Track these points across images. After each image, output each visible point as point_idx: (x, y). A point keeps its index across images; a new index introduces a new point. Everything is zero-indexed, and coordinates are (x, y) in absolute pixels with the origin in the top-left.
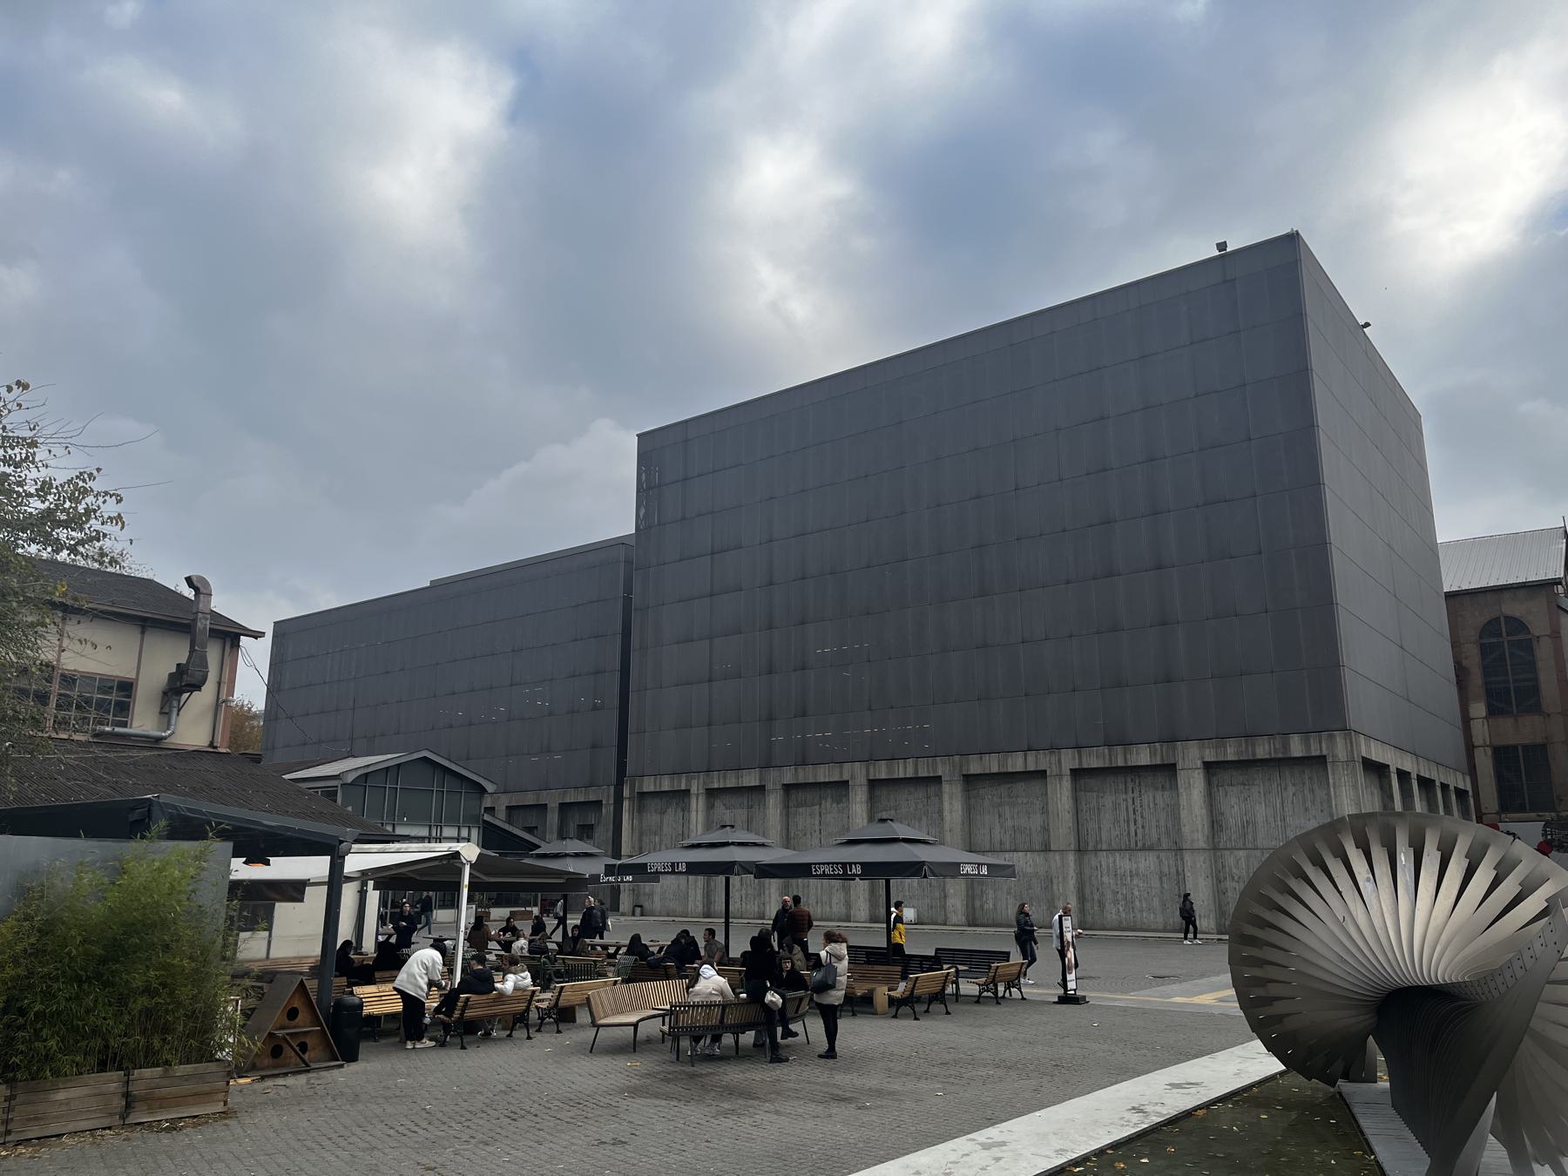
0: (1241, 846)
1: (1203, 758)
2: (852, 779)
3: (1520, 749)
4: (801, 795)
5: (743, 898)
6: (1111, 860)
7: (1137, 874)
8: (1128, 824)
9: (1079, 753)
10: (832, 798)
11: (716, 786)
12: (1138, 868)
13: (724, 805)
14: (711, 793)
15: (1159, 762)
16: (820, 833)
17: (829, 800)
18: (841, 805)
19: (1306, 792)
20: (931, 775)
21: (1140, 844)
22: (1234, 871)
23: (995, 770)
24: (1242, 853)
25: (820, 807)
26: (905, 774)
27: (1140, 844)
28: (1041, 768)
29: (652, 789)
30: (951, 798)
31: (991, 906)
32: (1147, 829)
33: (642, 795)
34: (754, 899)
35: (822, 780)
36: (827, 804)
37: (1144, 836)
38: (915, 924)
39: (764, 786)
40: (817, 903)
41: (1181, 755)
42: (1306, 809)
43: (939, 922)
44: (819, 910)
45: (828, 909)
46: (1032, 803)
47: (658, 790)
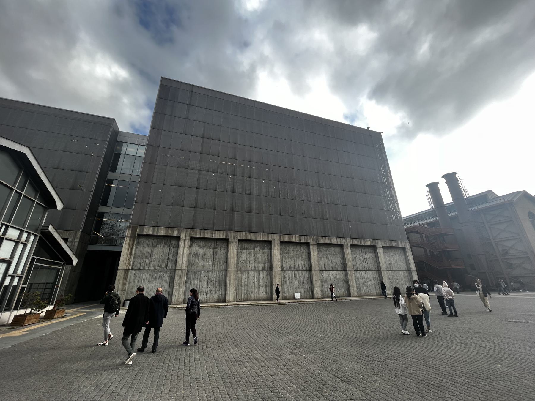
0: (390, 270)
1: (382, 245)
2: (273, 240)
4: (244, 245)
5: (209, 293)
6: (361, 274)
9: (352, 239)
10: (260, 247)
11: (198, 236)
12: (368, 276)
13: (199, 246)
15: (372, 245)
16: (254, 262)
17: (259, 248)
18: (264, 251)
20: (306, 242)
21: (367, 269)
22: (390, 277)
23: (328, 242)
24: (390, 272)
25: (254, 251)
26: (296, 240)
27: (367, 269)
28: (342, 243)
30: (313, 251)
31: (326, 290)
32: (368, 264)
33: (140, 236)
34: (216, 292)
35: (259, 239)
36: (258, 250)
37: (368, 266)
38: (301, 299)
39: (228, 239)
40: (252, 292)
41: (377, 243)
42: (401, 260)
43: (308, 297)
44: (253, 296)
45: (258, 295)
46: (337, 254)
47: (155, 234)
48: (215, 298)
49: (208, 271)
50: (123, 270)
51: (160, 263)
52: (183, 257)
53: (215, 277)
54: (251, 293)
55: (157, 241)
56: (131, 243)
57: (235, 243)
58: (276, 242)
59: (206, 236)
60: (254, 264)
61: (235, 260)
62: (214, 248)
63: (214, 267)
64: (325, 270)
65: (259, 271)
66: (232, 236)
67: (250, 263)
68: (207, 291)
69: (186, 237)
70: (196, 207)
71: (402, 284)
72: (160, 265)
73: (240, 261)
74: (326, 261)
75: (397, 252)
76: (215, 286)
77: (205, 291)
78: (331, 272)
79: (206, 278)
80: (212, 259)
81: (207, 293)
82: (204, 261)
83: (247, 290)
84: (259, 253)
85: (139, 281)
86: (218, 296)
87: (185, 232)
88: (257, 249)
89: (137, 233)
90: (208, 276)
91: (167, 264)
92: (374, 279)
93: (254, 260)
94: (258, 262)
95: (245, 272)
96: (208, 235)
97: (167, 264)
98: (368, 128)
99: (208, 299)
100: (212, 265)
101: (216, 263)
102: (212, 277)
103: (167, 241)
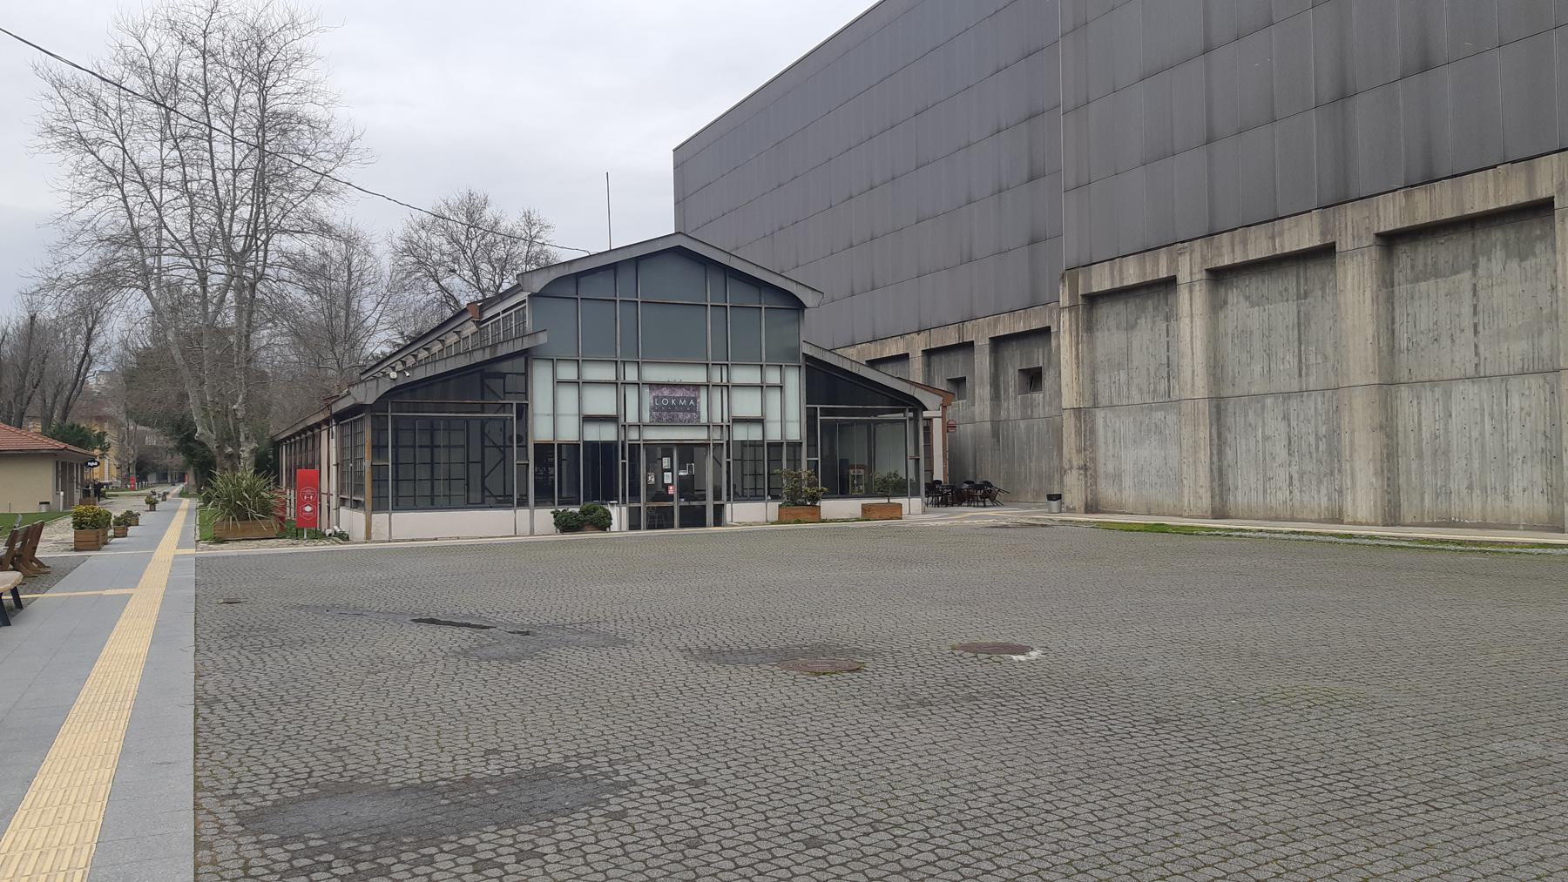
2: (1561, 190)
5: (1295, 482)
10: (1506, 246)
13: (1247, 298)
14: (1219, 276)
16: (1476, 332)
17: (1499, 254)
25: (1474, 275)
29: (1107, 286)
33: (1092, 299)
34: (1320, 482)
40: (1470, 487)
44: (1477, 505)
45: (1500, 502)
47: (1117, 285)
48: (1319, 505)
49: (1287, 395)
50: (1072, 411)
51: (1152, 380)
52: (1193, 354)
53: (1313, 422)
54: (1464, 492)
55: (1136, 305)
56: (1074, 327)
57: (1363, 255)
59: (1253, 256)
60: (1476, 346)
61: (1367, 340)
62: (1298, 298)
63: (1304, 378)
65: (1505, 377)
66: (1349, 224)
67: (1453, 341)
68: (1291, 477)
69: (1191, 274)
70: (1209, 141)
72: (1152, 388)
73: (1409, 339)
76: (1314, 455)
77: (1282, 475)
79: (1282, 426)
80: (1296, 344)
81: (1291, 484)
82: (1269, 356)
83: (1447, 477)
84: (1500, 285)
85: (1114, 441)
86: (1329, 499)
87: (1187, 255)
88: (1489, 260)
89: (1080, 293)
90: (1289, 415)
91: (1169, 380)
93: (1475, 326)
94: (1498, 334)
95: (1433, 391)
96: (1259, 247)
97: (1169, 380)
99: (1297, 504)
100: (1297, 371)
101: (1312, 360)
102: (1302, 417)
103: (1159, 300)
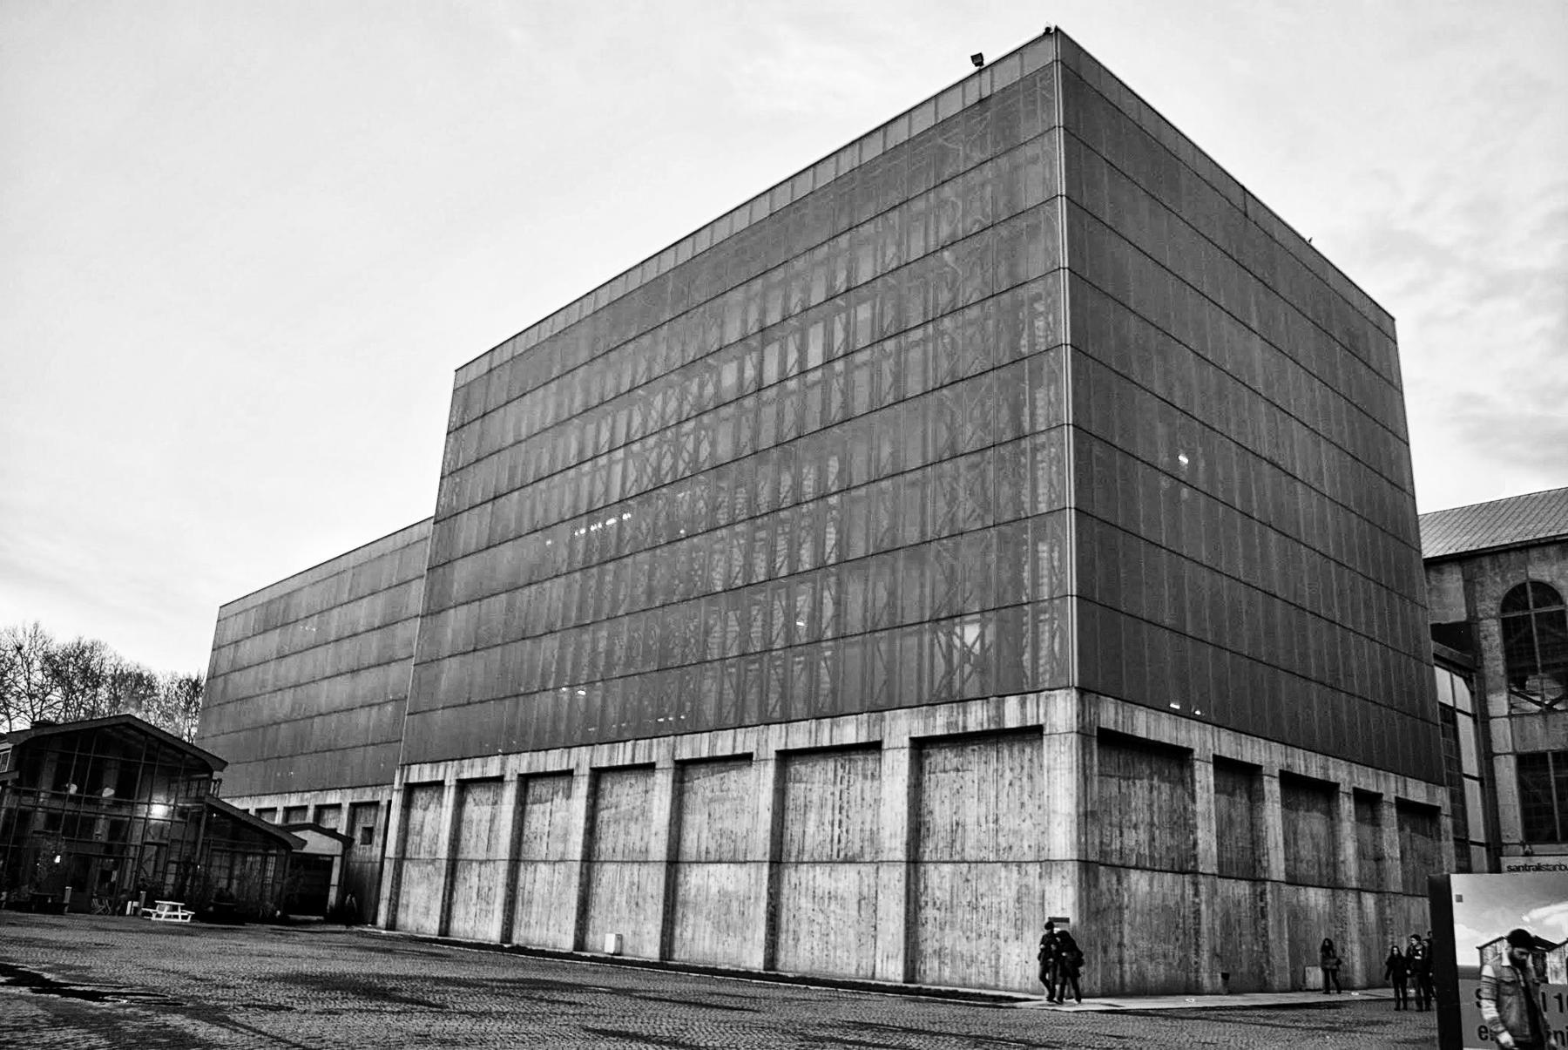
3: (1550, 755)
6: (811, 875)
7: (836, 897)
8: (833, 825)
19: (1025, 779)
21: (842, 854)
24: (947, 868)
27: (842, 854)
41: (887, 731)
42: (1023, 805)
58: (581, 772)
64: (698, 862)
71: (998, 937)
74: (706, 826)
75: (1011, 755)
78: (712, 868)
92: (859, 902)
98: (977, 59)
